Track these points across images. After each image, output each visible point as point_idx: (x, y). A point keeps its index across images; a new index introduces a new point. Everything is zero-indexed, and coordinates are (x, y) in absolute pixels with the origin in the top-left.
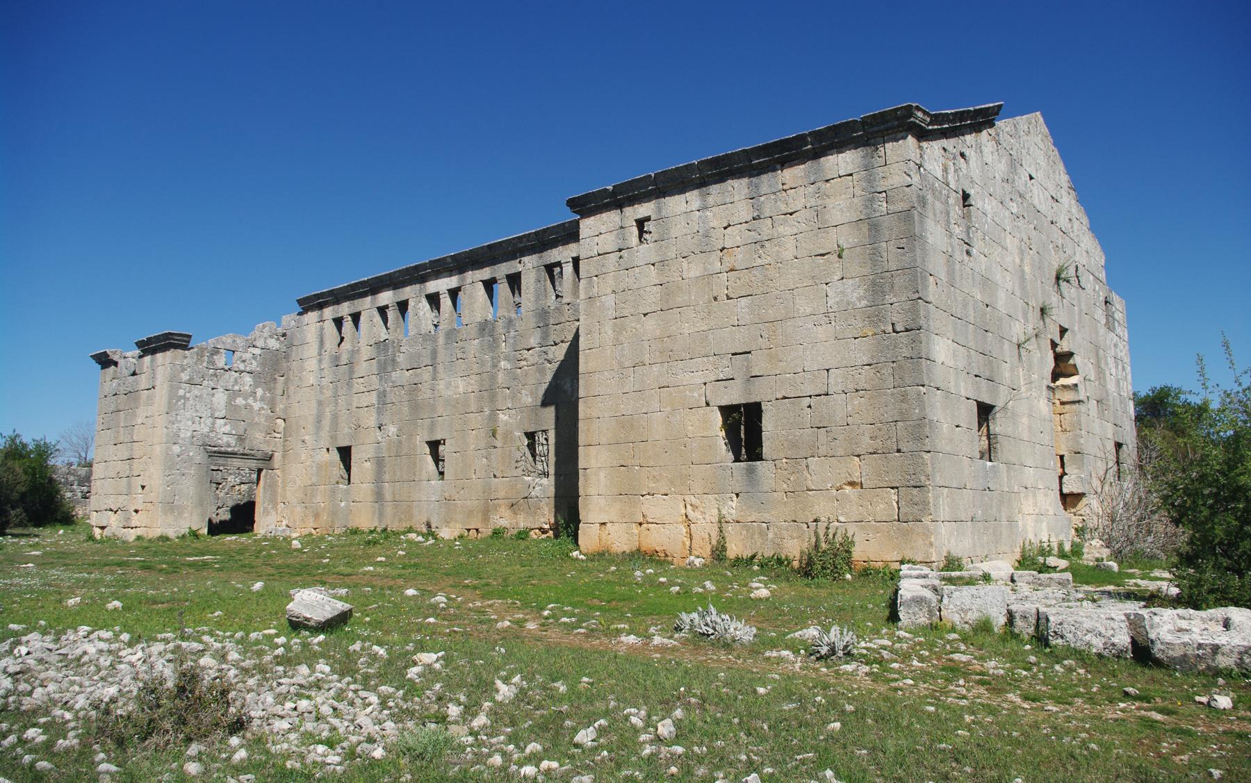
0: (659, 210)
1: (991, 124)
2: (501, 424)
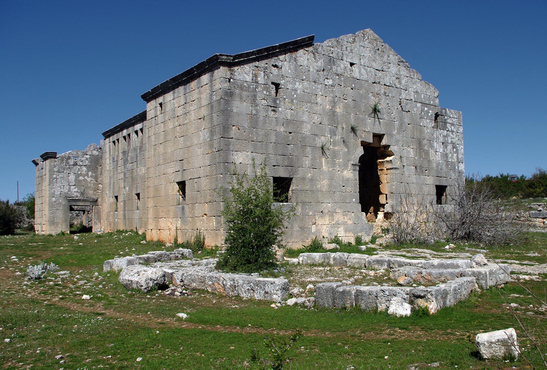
0: (164, 99)
1: (311, 45)
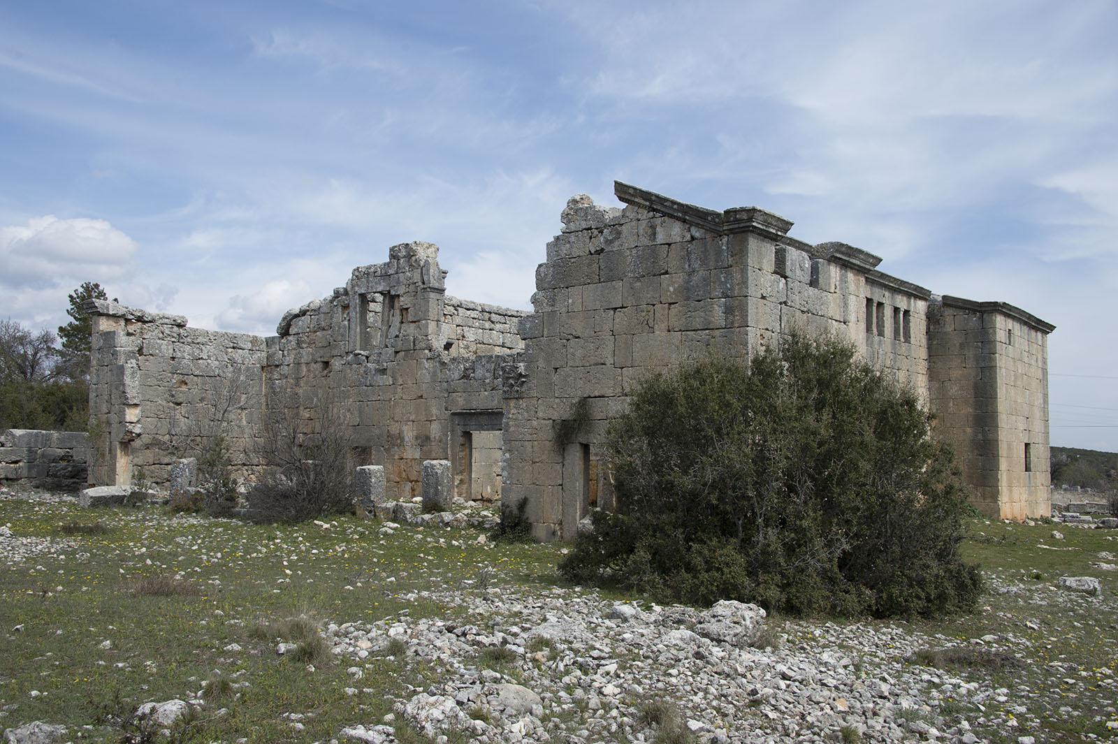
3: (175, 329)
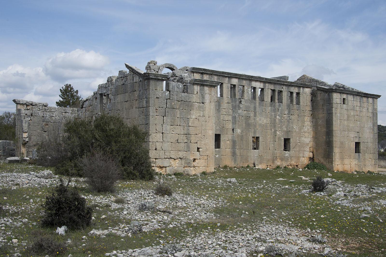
2: (278, 135)
3: (44, 107)
